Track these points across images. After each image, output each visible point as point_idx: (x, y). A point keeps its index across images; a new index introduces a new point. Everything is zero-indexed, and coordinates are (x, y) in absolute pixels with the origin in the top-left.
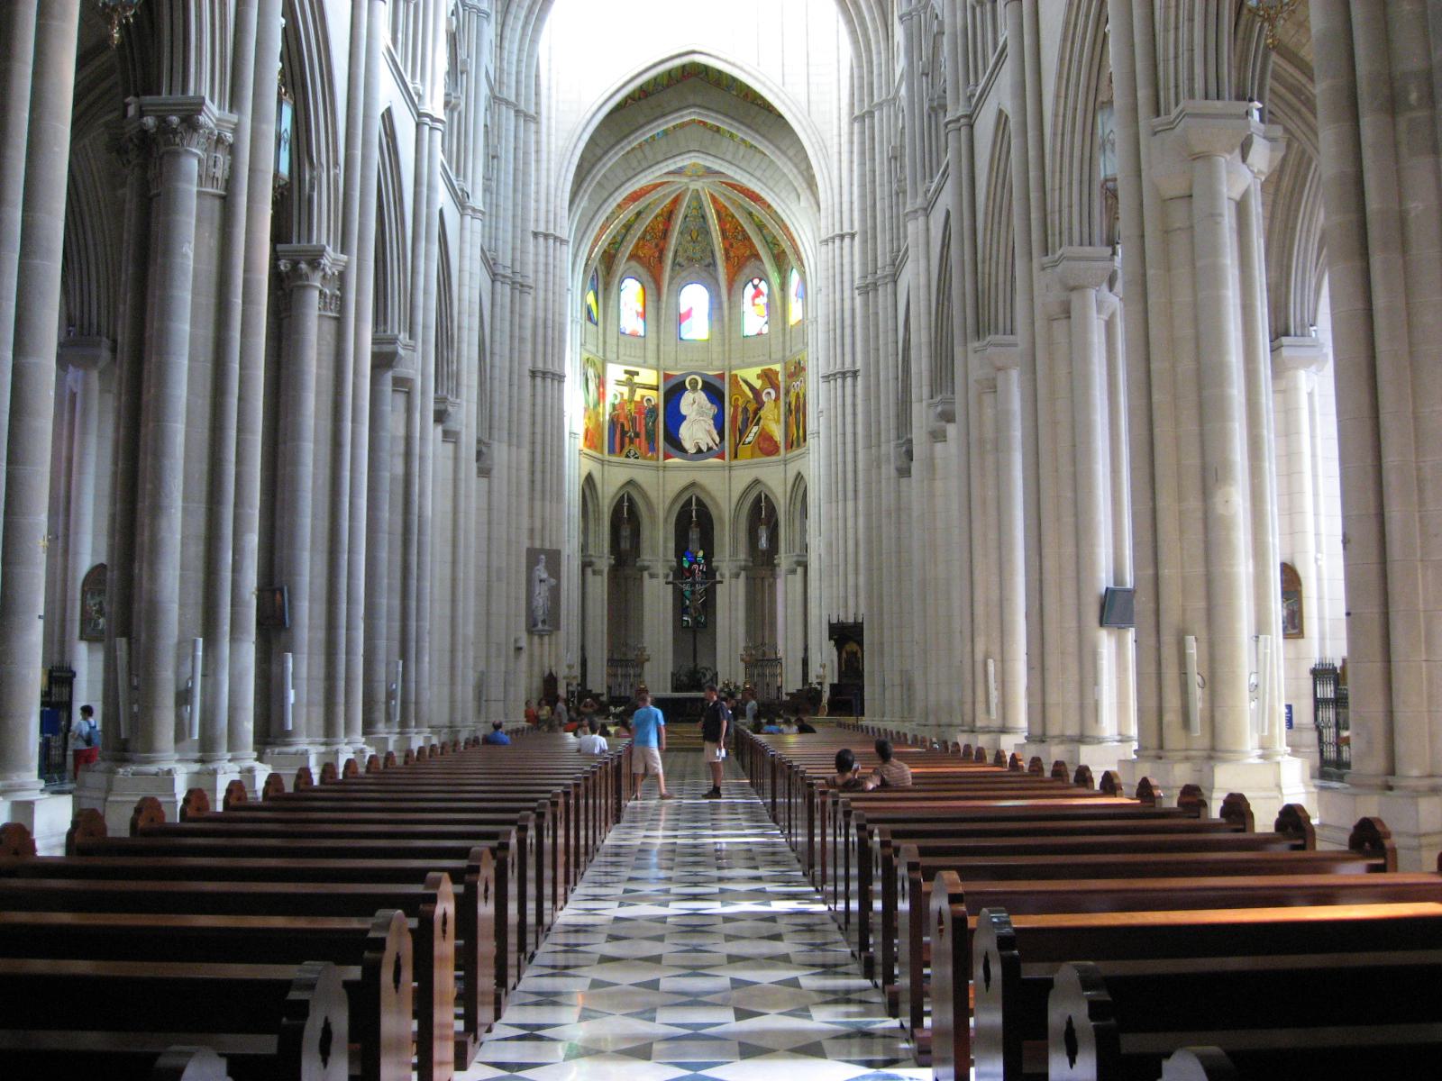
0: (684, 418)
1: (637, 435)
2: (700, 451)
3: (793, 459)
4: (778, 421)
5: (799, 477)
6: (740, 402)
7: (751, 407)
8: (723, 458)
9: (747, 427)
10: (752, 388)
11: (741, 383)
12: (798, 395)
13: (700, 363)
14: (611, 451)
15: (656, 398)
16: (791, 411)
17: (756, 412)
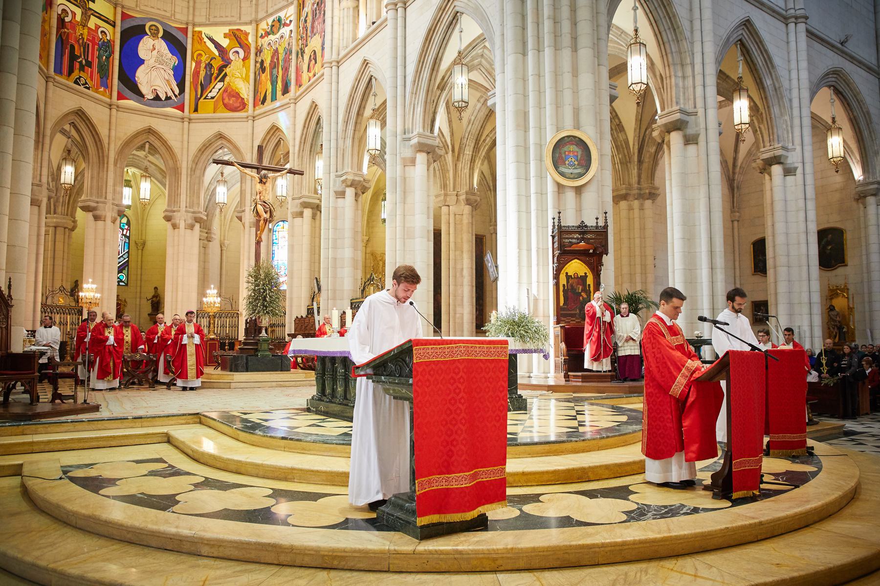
0: (142, 62)
1: (89, 64)
2: (157, 98)
3: (265, 114)
4: (246, 79)
5: (275, 129)
6: (203, 58)
7: (217, 64)
8: (181, 108)
9: (211, 82)
10: (217, 45)
11: (206, 40)
12: (276, 51)
13: (163, 13)
14: (58, 70)
15: (114, 35)
16: (263, 70)
17: (221, 69)
